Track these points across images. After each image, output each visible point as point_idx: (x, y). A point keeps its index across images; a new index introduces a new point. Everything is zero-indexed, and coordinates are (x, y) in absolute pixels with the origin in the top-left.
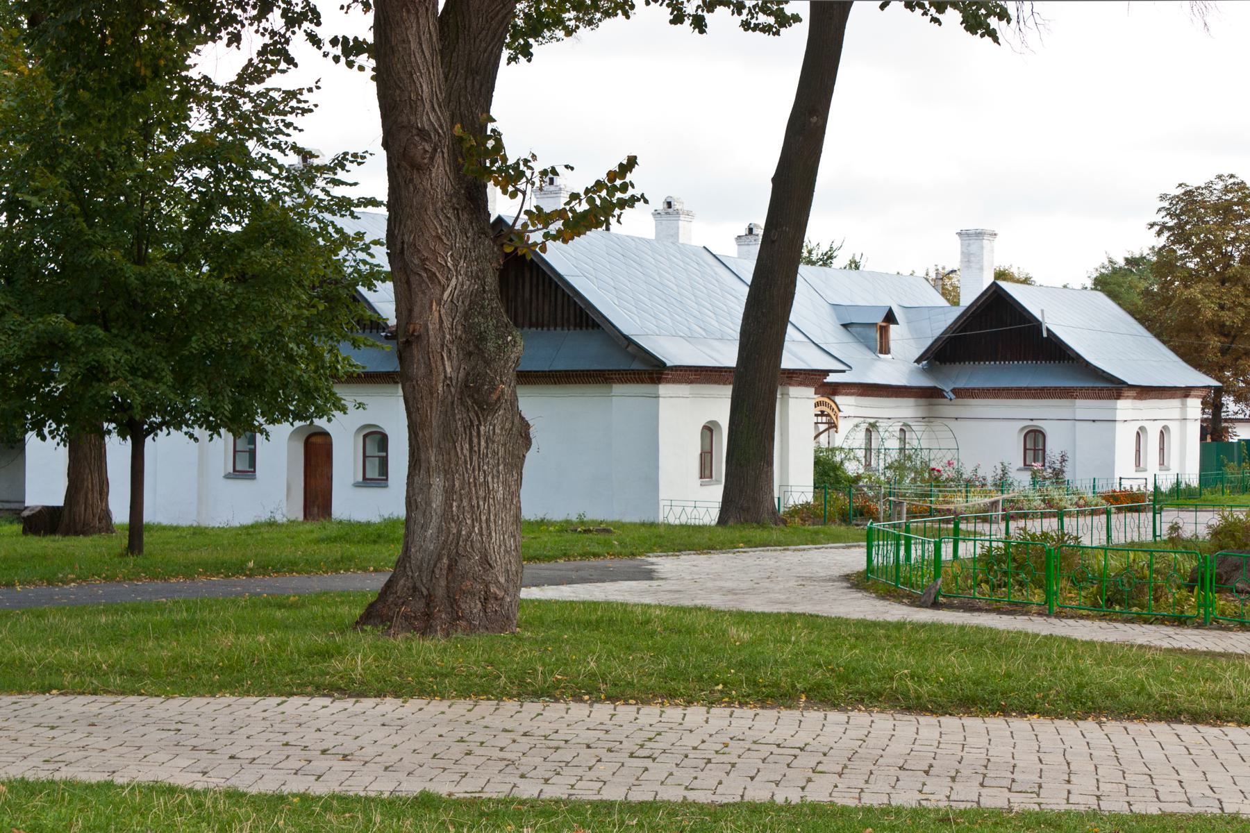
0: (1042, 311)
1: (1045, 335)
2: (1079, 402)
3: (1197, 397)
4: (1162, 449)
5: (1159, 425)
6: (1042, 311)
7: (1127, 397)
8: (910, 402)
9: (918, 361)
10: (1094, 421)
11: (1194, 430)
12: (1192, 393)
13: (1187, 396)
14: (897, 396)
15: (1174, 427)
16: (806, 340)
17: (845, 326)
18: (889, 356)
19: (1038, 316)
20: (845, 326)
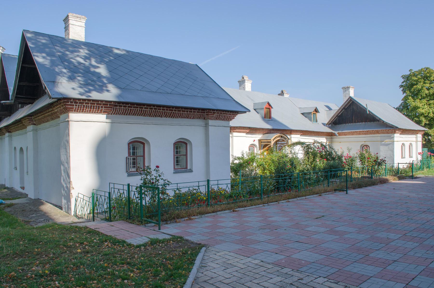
1: (368, 113)
3: (420, 134)
5: (409, 143)
6: (366, 105)
15: (414, 144)
17: (302, 114)
19: (366, 107)
20: (302, 114)
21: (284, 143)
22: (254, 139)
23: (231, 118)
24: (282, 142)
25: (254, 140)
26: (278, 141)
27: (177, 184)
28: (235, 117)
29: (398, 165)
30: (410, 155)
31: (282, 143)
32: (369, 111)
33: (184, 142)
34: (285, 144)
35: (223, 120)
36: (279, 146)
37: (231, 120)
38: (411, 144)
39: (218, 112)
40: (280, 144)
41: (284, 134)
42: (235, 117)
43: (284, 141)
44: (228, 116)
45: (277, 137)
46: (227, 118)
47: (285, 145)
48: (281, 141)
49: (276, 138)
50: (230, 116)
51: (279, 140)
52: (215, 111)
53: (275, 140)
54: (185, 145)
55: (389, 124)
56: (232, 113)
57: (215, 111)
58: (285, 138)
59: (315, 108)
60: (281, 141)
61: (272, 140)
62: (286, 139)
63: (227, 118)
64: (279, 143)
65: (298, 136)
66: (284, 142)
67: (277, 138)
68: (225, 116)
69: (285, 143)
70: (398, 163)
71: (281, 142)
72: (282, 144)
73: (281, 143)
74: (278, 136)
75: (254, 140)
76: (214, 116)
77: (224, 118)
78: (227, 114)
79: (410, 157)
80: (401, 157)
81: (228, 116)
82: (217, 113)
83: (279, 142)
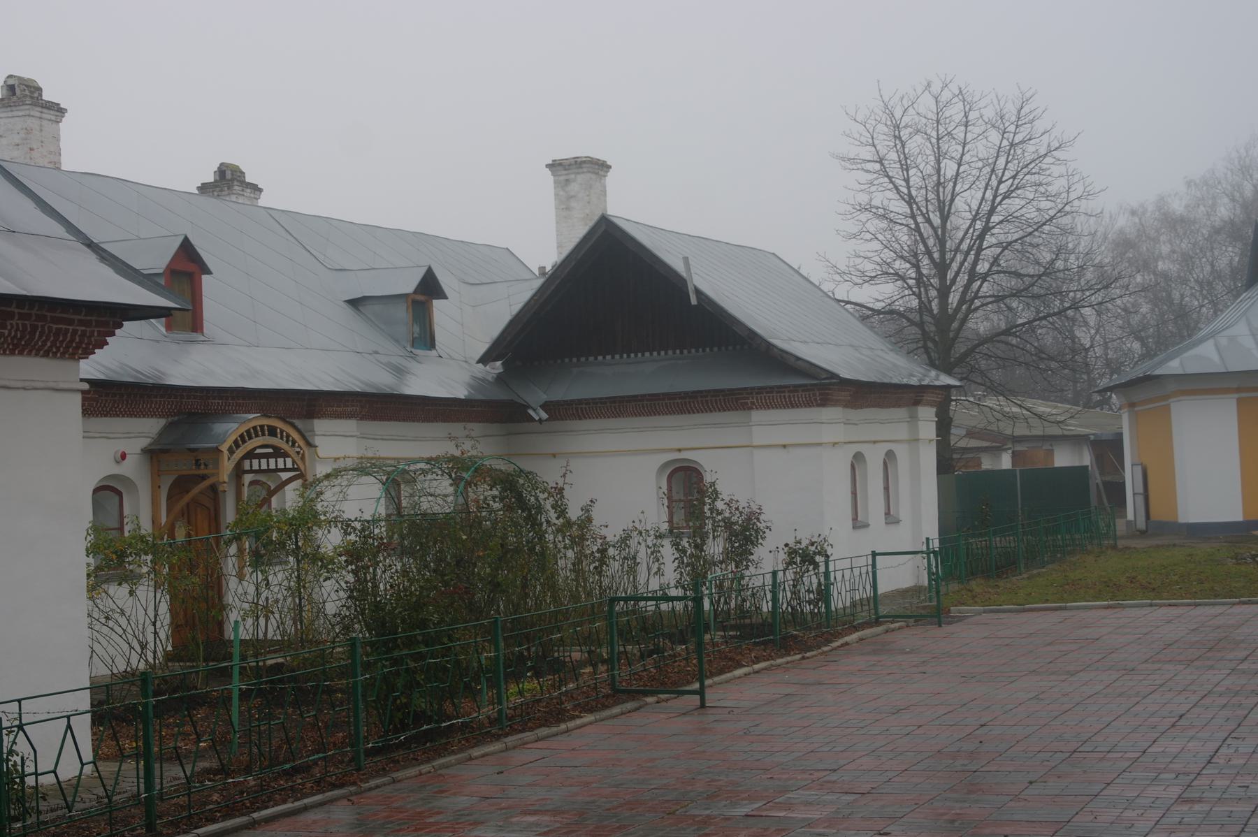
0: (686, 260)
1: (694, 301)
2: (757, 416)
3: (931, 404)
4: (887, 489)
5: (882, 449)
6: (686, 260)
7: (836, 403)
8: (477, 428)
9: (484, 360)
10: (784, 446)
11: (929, 458)
12: (927, 397)
13: (917, 403)
14: (446, 419)
15: (901, 452)
16: (60, 231)
17: (355, 303)
18: (434, 352)
19: (679, 267)
21: (281, 466)
22: (122, 446)
23: (88, 344)
24: (272, 461)
25: (123, 456)
26: (250, 455)
27: (19, 701)
28: (109, 339)
29: (874, 565)
30: (888, 514)
31: (272, 466)
32: (698, 292)
33: (103, 486)
34: (285, 470)
35: (46, 355)
36: (252, 483)
37: (87, 353)
38: (890, 455)
39: (25, 311)
40: (260, 471)
41: (283, 420)
42: (109, 339)
43: (285, 455)
44: (75, 332)
45: (248, 432)
46: (72, 341)
47: (285, 476)
48: (267, 456)
49: (244, 442)
50: (84, 333)
51: (255, 449)
52: (13, 309)
53: (239, 453)
54: (117, 499)
55: (798, 359)
56: (93, 318)
57: (13, 309)
58: (288, 436)
59: (422, 271)
60: (267, 456)
61: (226, 453)
62: (294, 442)
63: (72, 341)
64: (256, 467)
65: (350, 426)
66: (280, 461)
67: (250, 438)
68: (59, 330)
69: (289, 465)
70: (874, 554)
71: (264, 461)
72: (268, 471)
73: (264, 466)
74: (254, 428)
75: (123, 456)
76: (6, 332)
77: (53, 344)
78: (70, 322)
79: (891, 518)
80: (850, 523)
81: (75, 332)
82: (22, 317)
83: (255, 462)
